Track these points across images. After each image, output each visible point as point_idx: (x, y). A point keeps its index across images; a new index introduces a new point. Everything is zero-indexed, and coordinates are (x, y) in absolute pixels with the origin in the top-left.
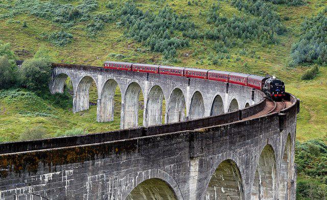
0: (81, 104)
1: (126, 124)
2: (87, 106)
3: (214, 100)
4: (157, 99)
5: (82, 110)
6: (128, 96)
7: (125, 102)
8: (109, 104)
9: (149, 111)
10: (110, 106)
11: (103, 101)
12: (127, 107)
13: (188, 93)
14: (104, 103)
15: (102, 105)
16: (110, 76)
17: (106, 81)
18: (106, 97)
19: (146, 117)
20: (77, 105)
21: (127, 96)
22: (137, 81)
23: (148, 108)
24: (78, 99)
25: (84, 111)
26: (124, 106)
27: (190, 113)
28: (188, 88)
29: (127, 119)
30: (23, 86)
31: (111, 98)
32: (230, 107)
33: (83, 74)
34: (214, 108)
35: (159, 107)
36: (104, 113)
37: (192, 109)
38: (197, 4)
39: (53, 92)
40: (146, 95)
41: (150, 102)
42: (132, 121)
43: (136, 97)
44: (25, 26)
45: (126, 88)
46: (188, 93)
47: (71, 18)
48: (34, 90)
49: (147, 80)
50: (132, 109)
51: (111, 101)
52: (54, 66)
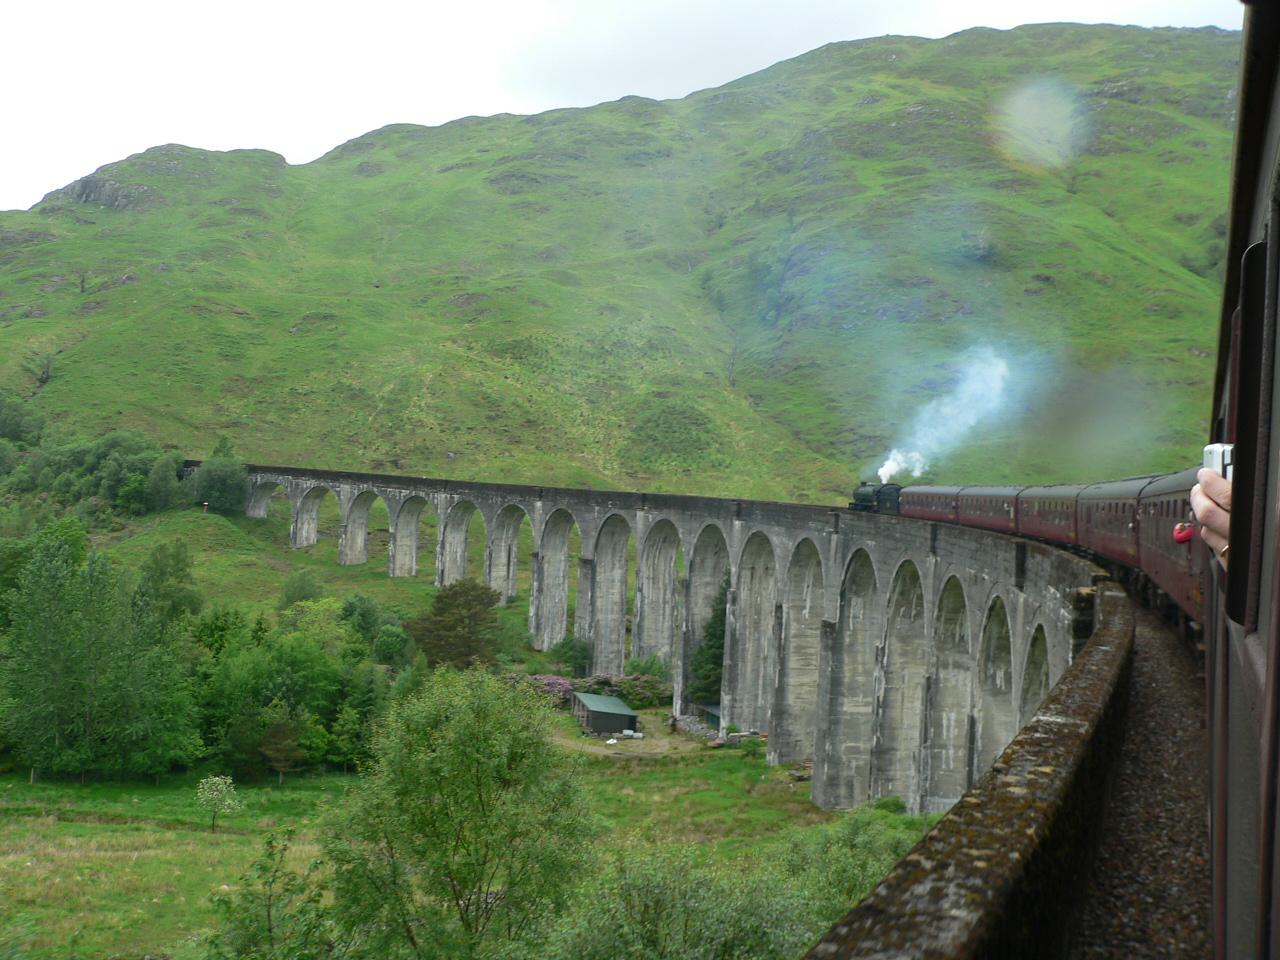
0: (304, 534)
1: (398, 566)
2: (313, 538)
3: (604, 523)
4: (459, 525)
5: (305, 544)
6: (401, 519)
9: (447, 546)
11: (350, 528)
12: (398, 539)
15: (349, 535)
16: (364, 487)
17: (356, 494)
18: (354, 521)
19: (442, 555)
22: (422, 494)
24: (299, 525)
25: (312, 546)
26: (394, 536)
27: (542, 546)
28: (539, 504)
29: (399, 558)
33: (309, 483)
35: (463, 539)
36: (351, 548)
37: (545, 539)
41: (448, 529)
42: (407, 563)
43: (414, 521)
49: (445, 492)
50: (407, 541)
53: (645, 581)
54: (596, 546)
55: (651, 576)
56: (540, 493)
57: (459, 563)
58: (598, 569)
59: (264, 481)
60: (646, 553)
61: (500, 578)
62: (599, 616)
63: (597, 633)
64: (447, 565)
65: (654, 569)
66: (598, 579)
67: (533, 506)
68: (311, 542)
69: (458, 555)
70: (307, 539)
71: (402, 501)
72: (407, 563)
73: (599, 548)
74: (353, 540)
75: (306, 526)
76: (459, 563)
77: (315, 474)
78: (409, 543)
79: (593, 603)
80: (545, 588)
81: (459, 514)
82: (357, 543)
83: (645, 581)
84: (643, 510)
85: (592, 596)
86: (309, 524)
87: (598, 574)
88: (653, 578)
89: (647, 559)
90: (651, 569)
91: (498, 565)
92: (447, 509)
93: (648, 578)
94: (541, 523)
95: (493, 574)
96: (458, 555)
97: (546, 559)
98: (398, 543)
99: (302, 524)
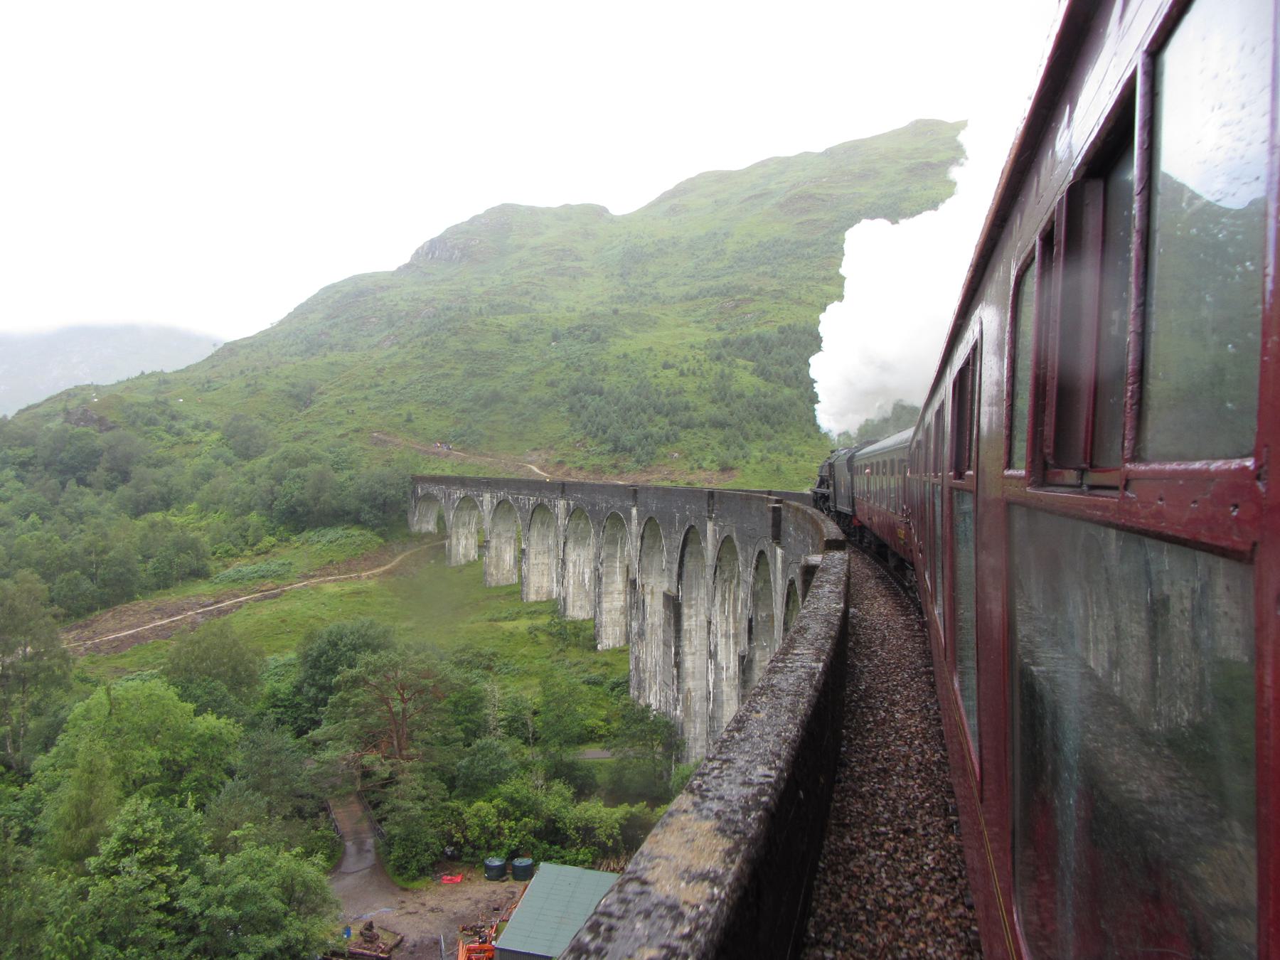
0: (461, 550)
4: (586, 538)
5: (463, 562)
6: (534, 534)
7: (529, 546)
8: (509, 549)
9: (570, 566)
10: (509, 556)
11: (493, 543)
12: (532, 556)
13: (635, 522)
14: (496, 548)
20: (454, 552)
21: (532, 531)
23: (567, 557)
24: (454, 541)
30: (357, 521)
31: (511, 538)
32: (719, 559)
33: (459, 493)
34: (687, 559)
35: (591, 556)
36: (497, 567)
38: (694, 373)
39: (415, 529)
40: (562, 529)
41: (570, 545)
42: (545, 585)
44: (409, 420)
45: (529, 517)
46: (635, 522)
47: (485, 406)
48: (373, 528)
51: (510, 544)
52: (417, 480)
53: (721, 642)
54: (680, 576)
55: (732, 632)
56: (634, 493)
57: (587, 587)
58: (685, 611)
59: (425, 492)
60: (719, 588)
61: (616, 610)
62: (690, 684)
63: (686, 710)
64: (571, 589)
65: (735, 618)
66: (686, 625)
67: (630, 514)
68: (471, 558)
69: (587, 577)
70: (465, 556)
71: (530, 512)
72: (545, 585)
73: (684, 577)
74: (499, 557)
75: (463, 542)
76: (587, 587)
77: (462, 482)
78: (546, 561)
79: (678, 665)
80: (648, 631)
81: (582, 525)
82: (504, 561)
83: (721, 642)
84: (710, 518)
85: (677, 654)
86: (467, 538)
87: (685, 618)
88: (736, 636)
89: (723, 604)
90: (731, 620)
91: (612, 593)
92: (565, 519)
93: (726, 636)
94: (637, 538)
95: (605, 605)
96: (587, 577)
97: (648, 589)
98: (533, 561)
99: (458, 539)
